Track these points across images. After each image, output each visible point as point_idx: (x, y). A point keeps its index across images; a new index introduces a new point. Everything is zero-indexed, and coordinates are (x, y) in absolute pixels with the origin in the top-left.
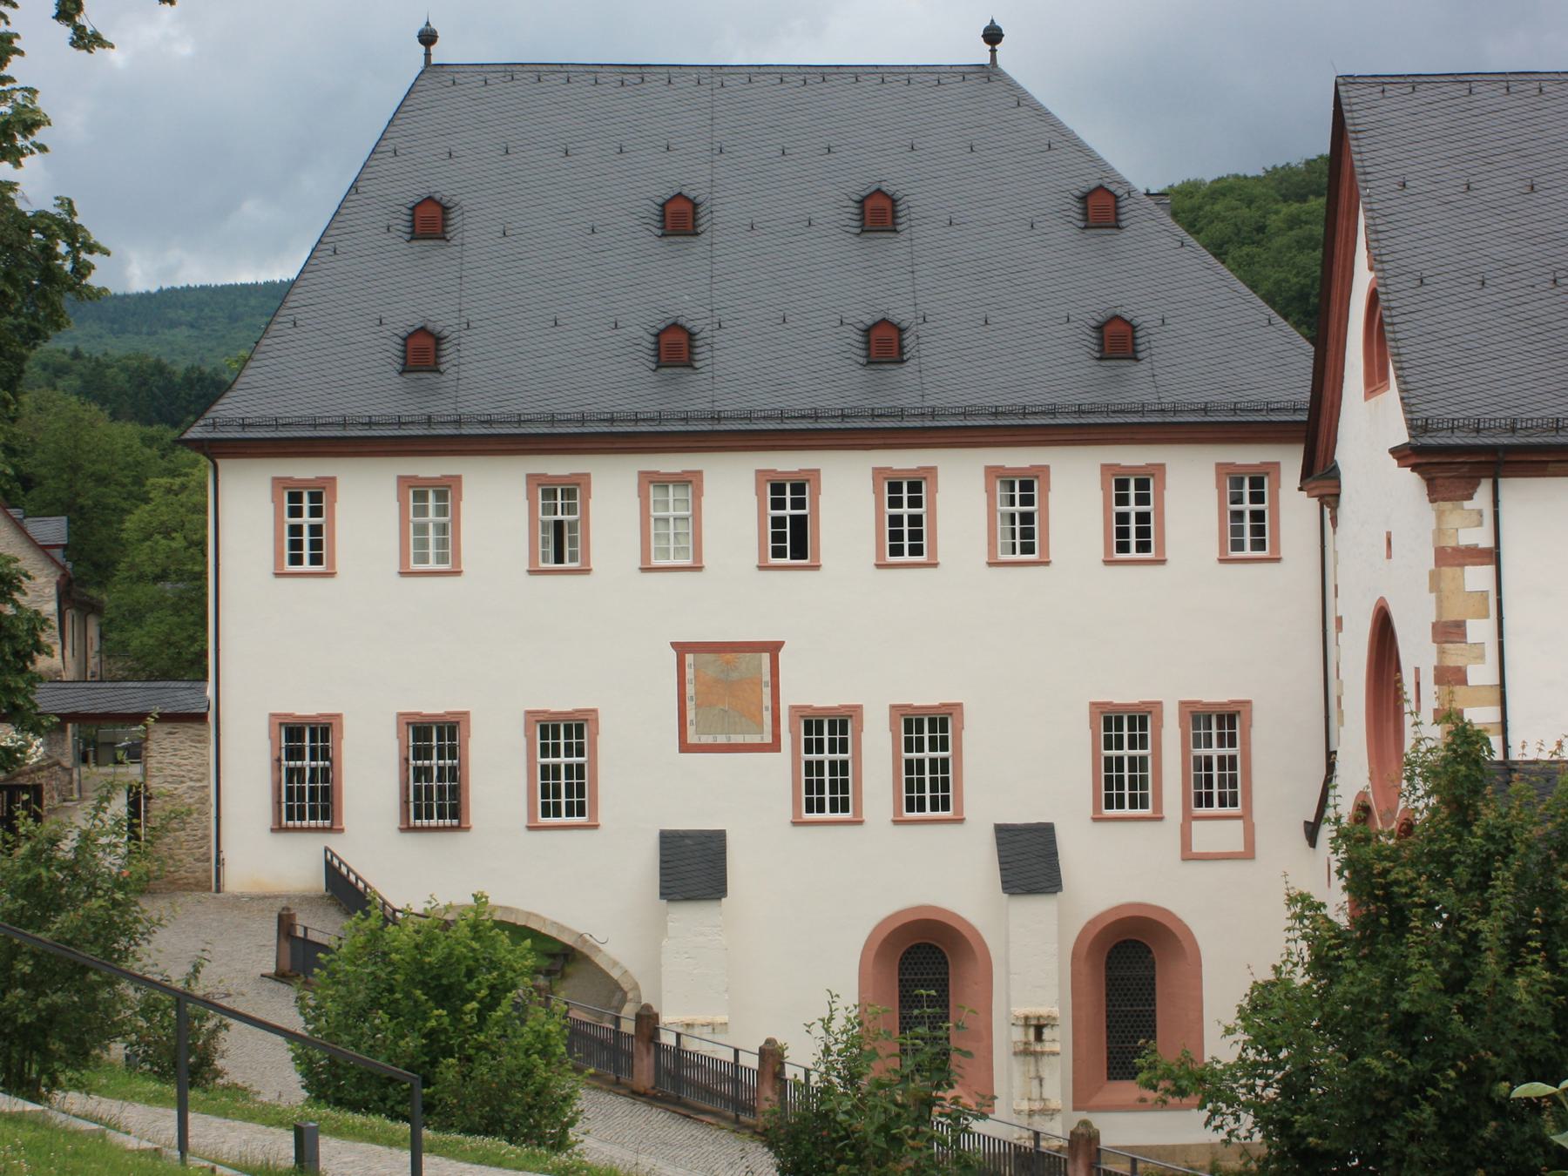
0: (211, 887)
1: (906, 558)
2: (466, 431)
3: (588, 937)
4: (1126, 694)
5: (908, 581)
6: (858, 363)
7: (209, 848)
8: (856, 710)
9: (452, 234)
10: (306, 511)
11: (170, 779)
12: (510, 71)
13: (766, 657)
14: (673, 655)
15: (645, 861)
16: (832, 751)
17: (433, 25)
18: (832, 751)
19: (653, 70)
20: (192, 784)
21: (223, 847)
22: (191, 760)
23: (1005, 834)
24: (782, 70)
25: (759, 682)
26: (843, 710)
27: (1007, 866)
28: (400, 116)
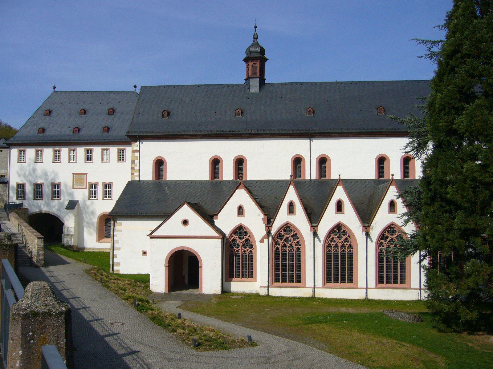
8: (98, 183)
13: (85, 175)
14: (72, 175)
16: (94, 189)
18: (94, 189)
25: (84, 179)
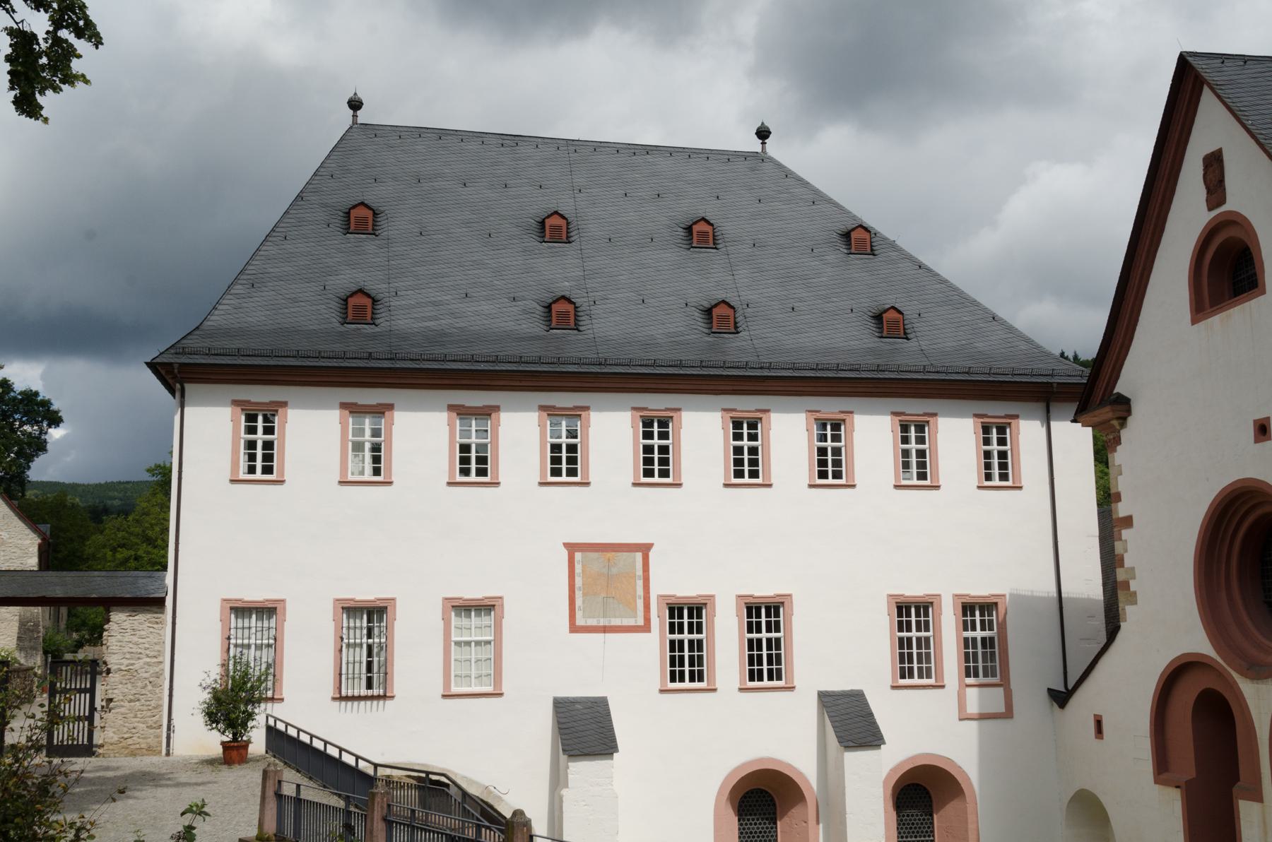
0: (160, 752)
1: (746, 480)
2: (399, 365)
3: (492, 789)
4: (914, 590)
5: (748, 497)
6: (704, 332)
7: (161, 717)
9: (379, 232)
10: (260, 430)
11: (128, 656)
12: (420, 132)
13: (639, 556)
14: (565, 553)
15: (543, 724)
16: (691, 632)
17: (360, 95)
18: (691, 632)
19: (525, 139)
20: (148, 660)
21: (174, 716)
22: (148, 639)
23: (827, 700)
24: (618, 146)
26: (700, 599)
27: (837, 724)
28: (335, 153)
